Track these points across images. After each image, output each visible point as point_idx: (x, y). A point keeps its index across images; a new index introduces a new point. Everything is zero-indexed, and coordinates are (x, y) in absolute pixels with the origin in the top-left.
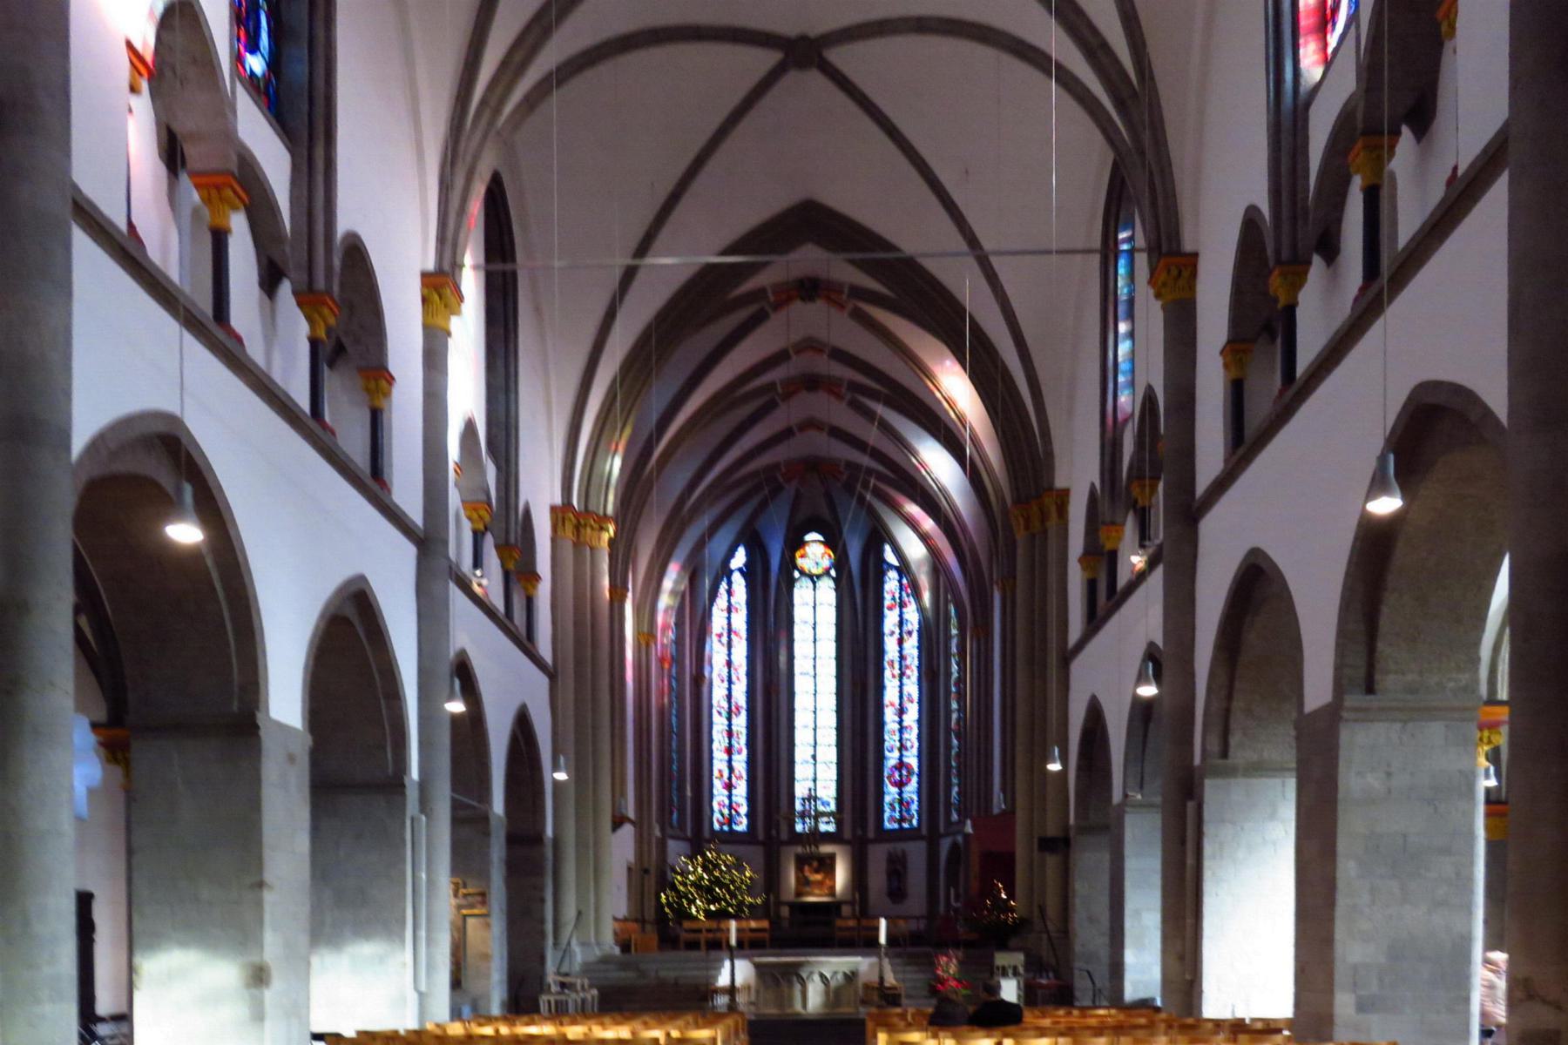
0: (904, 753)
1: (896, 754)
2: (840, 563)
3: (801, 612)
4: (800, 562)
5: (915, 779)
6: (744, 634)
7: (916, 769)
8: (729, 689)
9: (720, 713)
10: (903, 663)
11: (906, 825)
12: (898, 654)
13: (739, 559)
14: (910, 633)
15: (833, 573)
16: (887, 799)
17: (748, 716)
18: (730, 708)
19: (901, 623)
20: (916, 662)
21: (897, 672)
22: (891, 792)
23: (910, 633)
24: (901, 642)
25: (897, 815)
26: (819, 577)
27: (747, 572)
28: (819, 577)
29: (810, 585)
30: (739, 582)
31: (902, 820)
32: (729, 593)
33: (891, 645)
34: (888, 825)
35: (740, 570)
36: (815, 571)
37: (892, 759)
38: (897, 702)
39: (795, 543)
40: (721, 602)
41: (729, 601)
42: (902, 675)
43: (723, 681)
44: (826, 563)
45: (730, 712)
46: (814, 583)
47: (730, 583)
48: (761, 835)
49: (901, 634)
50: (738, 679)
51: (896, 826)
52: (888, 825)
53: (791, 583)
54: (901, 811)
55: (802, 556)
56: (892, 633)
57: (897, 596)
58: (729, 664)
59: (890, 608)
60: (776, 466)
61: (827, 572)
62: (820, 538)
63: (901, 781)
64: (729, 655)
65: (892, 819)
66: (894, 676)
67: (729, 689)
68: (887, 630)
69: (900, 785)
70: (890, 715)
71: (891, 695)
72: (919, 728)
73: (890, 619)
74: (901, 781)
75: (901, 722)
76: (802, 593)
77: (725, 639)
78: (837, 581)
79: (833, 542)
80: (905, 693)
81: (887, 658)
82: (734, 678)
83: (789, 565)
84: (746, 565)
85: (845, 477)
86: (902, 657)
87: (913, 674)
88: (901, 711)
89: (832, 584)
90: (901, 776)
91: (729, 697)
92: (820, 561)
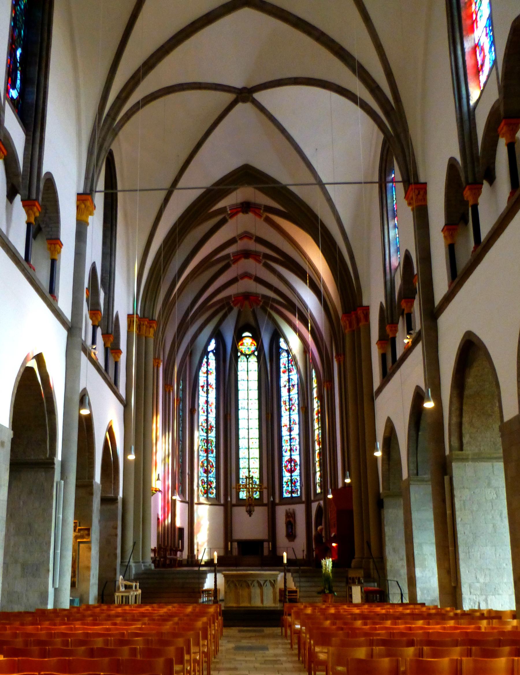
0: (292, 453)
1: (288, 453)
2: (260, 348)
3: (241, 375)
4: (241, 348)
5: (298, 468)
6: (214, 386)
7: (298, 463)
8: (207, 416)
9: (202, 430)
10: (291, 402)
11: (294, 495)
12: (288, 397)
13: (212, 346)
14: (293, 386)
15: (256, 353)
16: (285, 480)
17: (216, 431)
18: (207, 426)
19: (289, 380)
20: (297, 402)
21: (288, 407)
22: (286, 476)
23: (293, 386)
24: (289, 390)
25: (290, 489)
26: (250, 355)
27: (216, 353)
28: (250, 355)
29: (246, 360)
30: (211, 356)
31: (292, 492)
32: (208, 363)
33: (284, 392)
34: (286, 495)
35: (212, 351)
36: (248, 352)
37: (286, 457)
38: (288, 424)
39: (238, 338)
40: (204, 369)
41: (207, 368)
42: (290, 409)
43: (204, 412)
44: (253, 348)
45: (207, 429)
46: (247, 359)
47: (208, 359)
48: (222, 502)
49: (289, 386)
50: (211, 410)
51: (289, 495)
52: (286, 495)
53: (237, 358)
54: (292, 487)
55: (242, 345)
56: (285, 386)
57: (287, 365)
58: (207, 402)
59: (284, 372)
60: (229, 297)
61: (253, 353)
62: (250, 335)
63: (291, 468)
64: (207, 397)
65: (287, 492)
66: (286, 410)
67: (207, 416)
68: (282, 384)
69: (291, 471)
70: (285, 432)
71: (285, 421)
72: (300, 438)
73: (284, 378)
74: (291, 468)
75: (290, 435)
76: (242, 364)
77: (205, 389)
78: (258, 357)
79: (256, 337)
80: (292, 419)
81: (283, 399)
82: (209, 411)
83: (235, 350)
84: (215, 349)
85: (261, 303)
86: (290, 400)
87: (296, 408)
88: (290, 430)
89: (255, 359)
90: (291, 466)
91: (207, 420)
92: (250, 347)
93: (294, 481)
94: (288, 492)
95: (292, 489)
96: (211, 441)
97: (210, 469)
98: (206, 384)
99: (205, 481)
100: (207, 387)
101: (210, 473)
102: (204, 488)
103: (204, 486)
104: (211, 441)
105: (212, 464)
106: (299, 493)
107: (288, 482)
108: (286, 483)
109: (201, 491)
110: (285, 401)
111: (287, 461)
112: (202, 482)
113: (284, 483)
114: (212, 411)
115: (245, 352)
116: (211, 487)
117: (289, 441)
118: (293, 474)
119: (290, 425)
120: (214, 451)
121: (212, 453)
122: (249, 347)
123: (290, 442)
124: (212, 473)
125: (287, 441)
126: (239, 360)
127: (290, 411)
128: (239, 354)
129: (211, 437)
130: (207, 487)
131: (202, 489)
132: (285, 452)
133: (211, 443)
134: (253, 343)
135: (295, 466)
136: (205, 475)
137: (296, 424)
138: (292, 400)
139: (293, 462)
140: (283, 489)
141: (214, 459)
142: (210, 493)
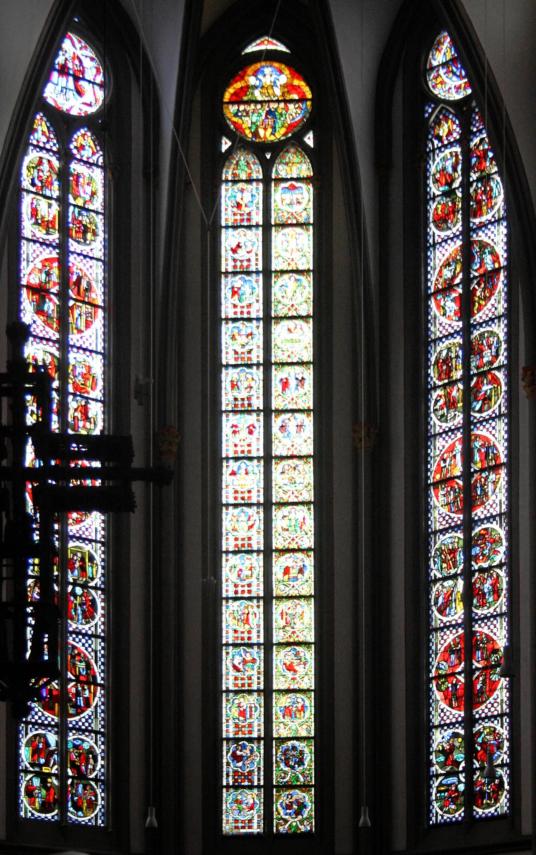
15: (309, 140)
21: (457, 392)
29: (257, 173)
50: (85, 410)
51: (459, 815)
54: (469, 771)
55: (237, 100)
56: (449, 287)
63: (470, 684)
66: (451, 404)
72: (512, 535)
74: (470, 684)
90: (469, 672)
93: (484, 744)
94: (454, 801)
95: (470, 783)
96: (83, 559)
97: (78, 694)
98: (55, 278)
99: (53, 746)
100: (63, 296)
101: (80, 710)
102: (44, 777)
103: (45, 770)
104: (83, 559)
105: (88, 666)
106: (504, 800)
107: (453, 748)
108: (442, 759)
109: (30, 792)
110: (447, 360)
111: (449, 650)
112: (36, 752)
113: (433, 757)
114: (90, 415)
115: (256, 134)
116: (81, 776)
117: (460, 557)
118: (480, 711)
119: (467, 474)
120: (100, 604)
121: (89, 616)
122: (273, 106)
123: (469, 558)
124: (89, 712)
125: (453, 552)
126: (228, 174)
127: (467, 410)
128: (226, 144)
129: (79, 538)
130: (62, 776)
131: (37, 782)
132: (441, 611)
133: (83, 569)
134: (296, 89)
135: (488, 668)
136: (52, 718)
137: (495, 468)
138: (480, 353)
139: (479, 654)
140: (431, 786)
141: (99, 645)
142: (77, 807)
